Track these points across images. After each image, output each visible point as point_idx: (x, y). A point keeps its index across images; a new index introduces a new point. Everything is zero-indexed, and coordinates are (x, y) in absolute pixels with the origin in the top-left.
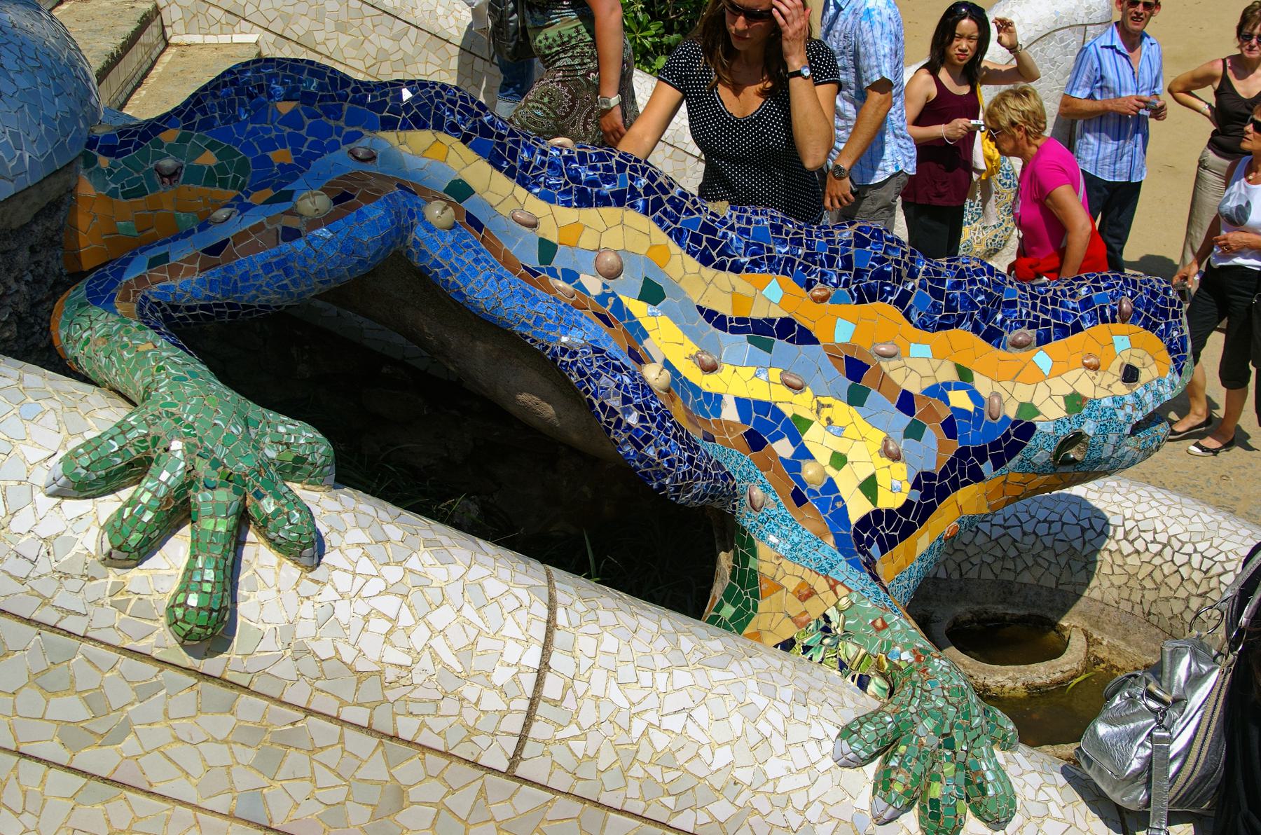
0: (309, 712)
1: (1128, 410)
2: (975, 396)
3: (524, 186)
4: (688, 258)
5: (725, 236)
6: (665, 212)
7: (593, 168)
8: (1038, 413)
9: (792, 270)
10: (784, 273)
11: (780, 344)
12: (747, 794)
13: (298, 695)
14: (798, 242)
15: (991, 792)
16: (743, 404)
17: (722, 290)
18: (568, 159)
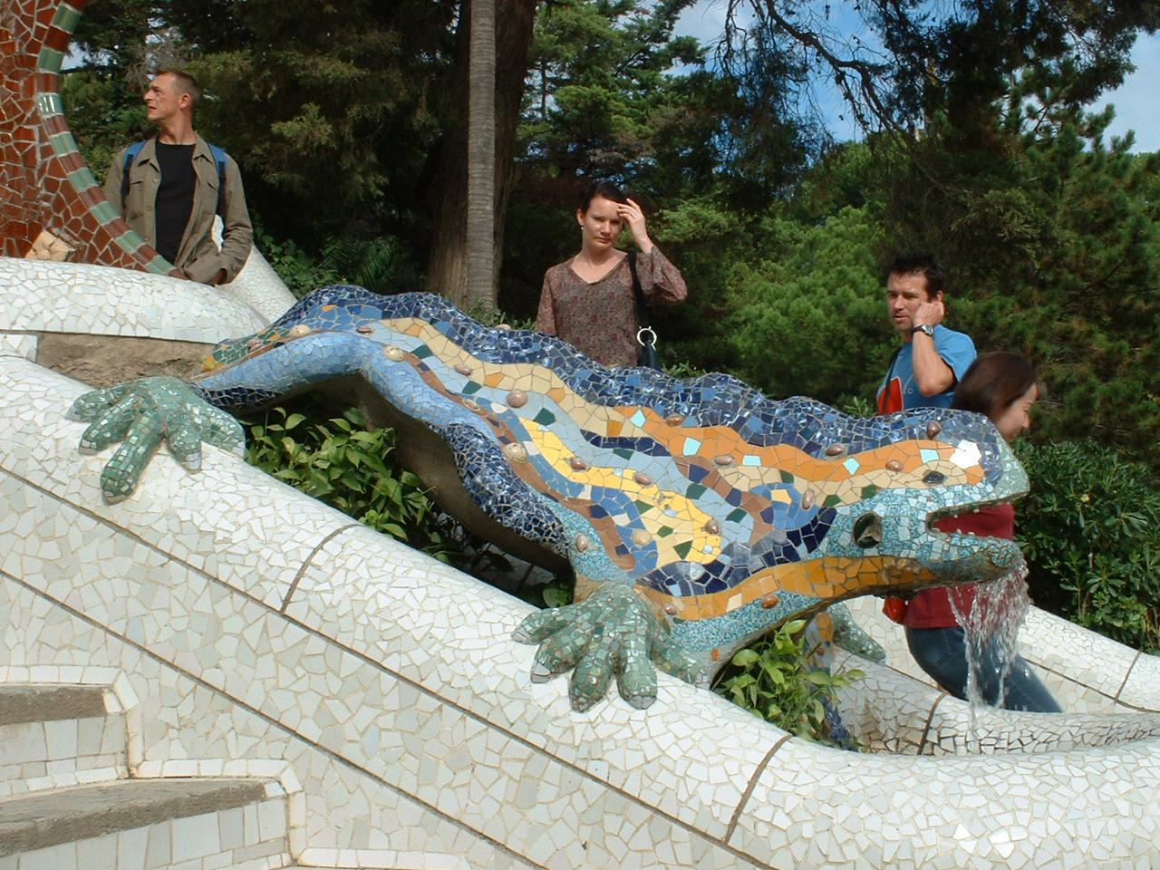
0: (171, 557)
2: (793, 494)
3: (467, 350)
4: (577, 396)
6: (564, 367)
7: (518, 340)
8: (839, 501)
9: (653, 404)
10: (647, 406)
12: (437, 647)
13: (165, 545)
14: (663, 386)
17: (599, 419)
18: (500, 336)
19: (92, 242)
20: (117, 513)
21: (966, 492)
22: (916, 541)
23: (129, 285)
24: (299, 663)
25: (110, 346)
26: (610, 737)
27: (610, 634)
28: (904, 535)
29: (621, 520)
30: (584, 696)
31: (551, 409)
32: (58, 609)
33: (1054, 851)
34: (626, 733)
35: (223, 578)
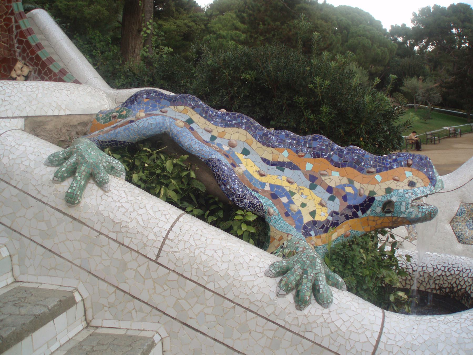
0: (101, 233)
1: (410, 194)
2: (354, 188)
3: (209, 121)
4: (258, 143)
5: (270, 137)
6: (252, 130)
7: (230, 117)
9: (292, 147)
10: (289, 148)
11: (287, 170)
12: (232, 279)
13: (97, 227)
15: (321, 292)
16: (272, 186)
17: (269, 153)
18: (223, 115)
19: (39, 67)
20: (72, 212)
21: (425, 190)
22: (407, 211)
23: (60, 91)
24: (165, 284)
26: (315, 322)
27: (311, 275)
29: (284, 200)
30: (301, 303)
31: (248, 148)
34: (322, 320)
35: (126, 244)
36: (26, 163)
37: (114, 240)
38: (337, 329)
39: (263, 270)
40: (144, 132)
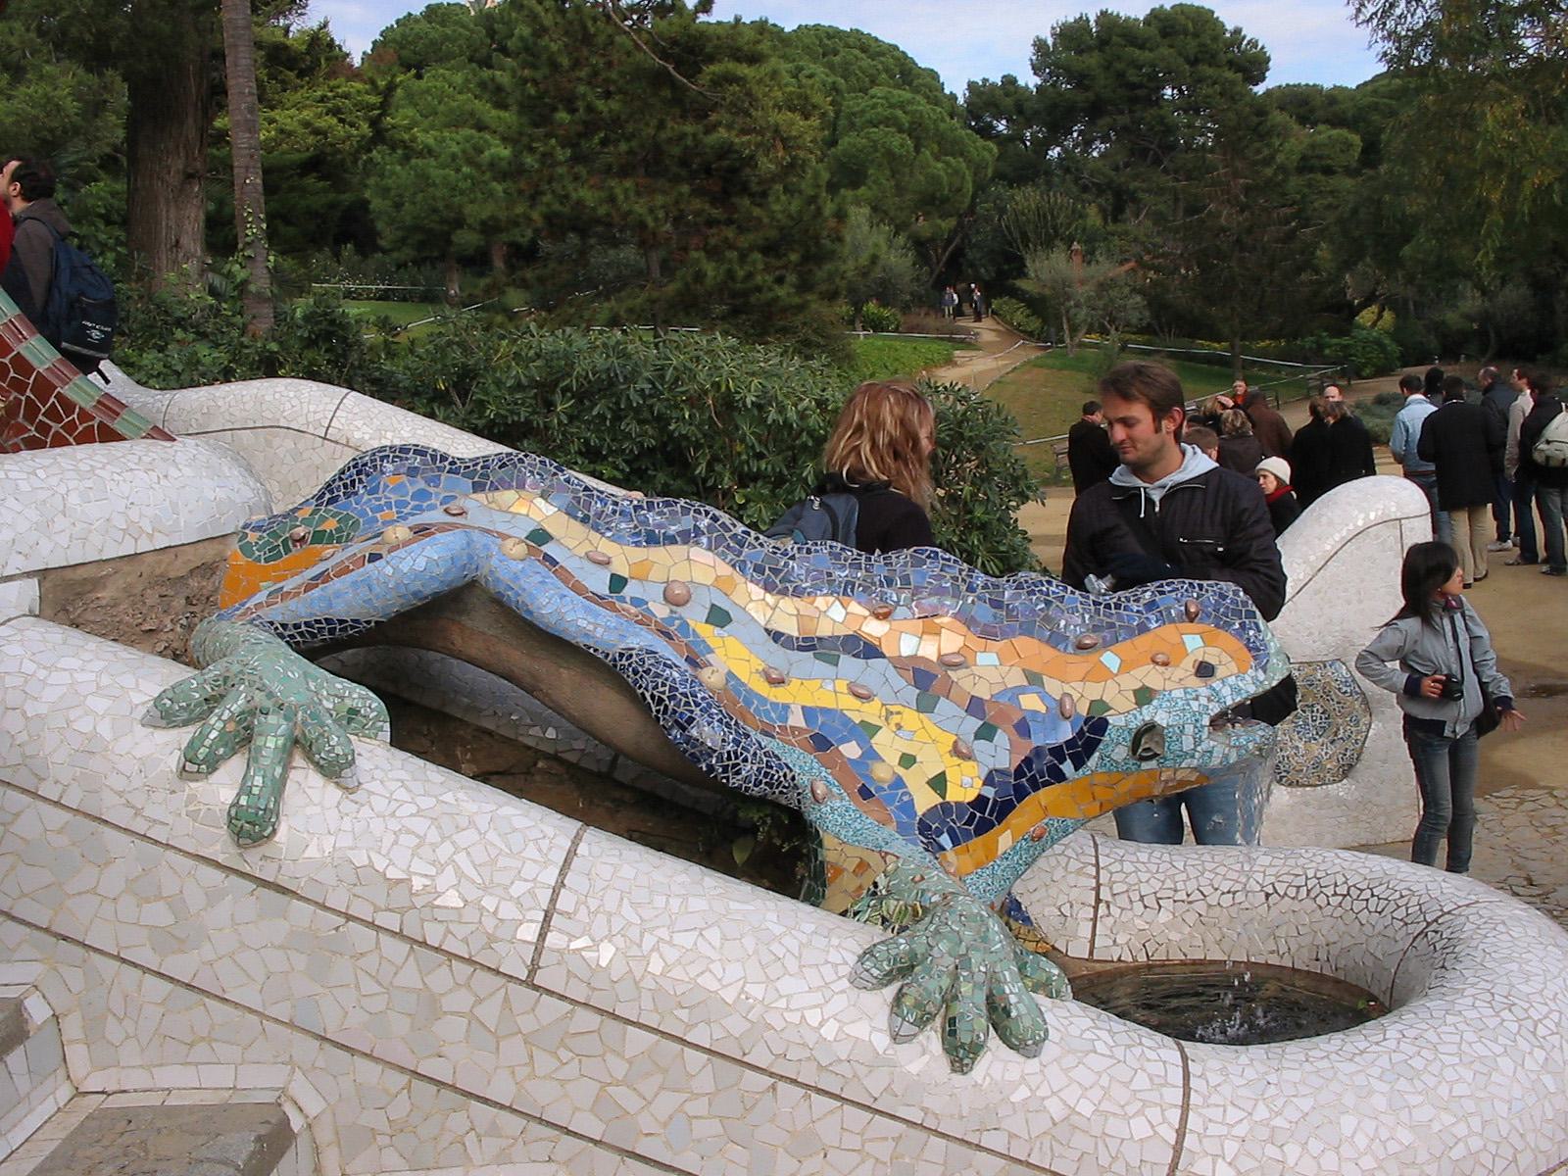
0: (349, 918)
1: (1203, 701)
2: (1044, 696)
3: (598, 531)
5: (786, 565)
6: (728, 547)
7: (661, 513)
10: (845, 593)
11: (845, 660)
13: (336, 901)
15: (1014, 1014)
16: (808, 712)
17: (787, 614)
18: (636, 508)
19: (28, 393)
20: (252, 861)
23: (128, 475)
24: (562, 1044)
25: (127, 568)
28: (1188, 743)
29: (851, 750)
30: (961, 1054)
31: (724, 605)
32: (182, 991)
33: (1509, 1153)
34: (1023, 1093)
36: (84, 726)
37: (393, 934)
38: (1067, 1111)
39: (845, 970)
40: (417, 586)
